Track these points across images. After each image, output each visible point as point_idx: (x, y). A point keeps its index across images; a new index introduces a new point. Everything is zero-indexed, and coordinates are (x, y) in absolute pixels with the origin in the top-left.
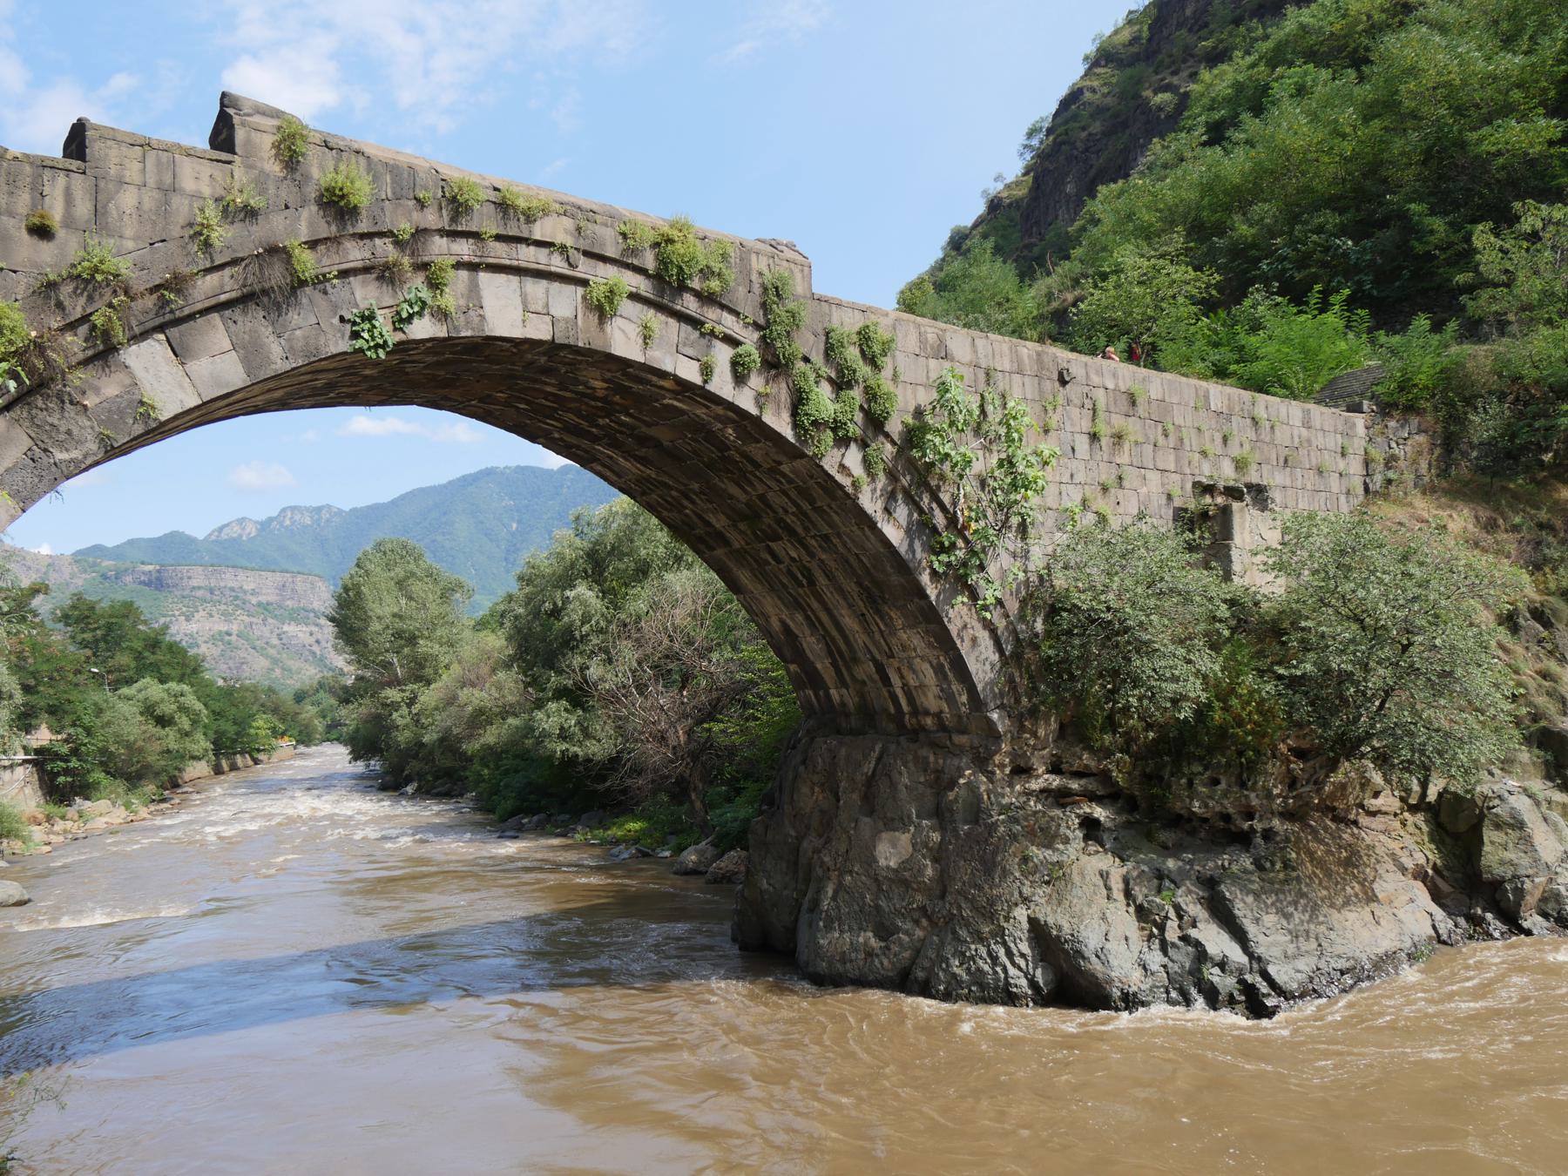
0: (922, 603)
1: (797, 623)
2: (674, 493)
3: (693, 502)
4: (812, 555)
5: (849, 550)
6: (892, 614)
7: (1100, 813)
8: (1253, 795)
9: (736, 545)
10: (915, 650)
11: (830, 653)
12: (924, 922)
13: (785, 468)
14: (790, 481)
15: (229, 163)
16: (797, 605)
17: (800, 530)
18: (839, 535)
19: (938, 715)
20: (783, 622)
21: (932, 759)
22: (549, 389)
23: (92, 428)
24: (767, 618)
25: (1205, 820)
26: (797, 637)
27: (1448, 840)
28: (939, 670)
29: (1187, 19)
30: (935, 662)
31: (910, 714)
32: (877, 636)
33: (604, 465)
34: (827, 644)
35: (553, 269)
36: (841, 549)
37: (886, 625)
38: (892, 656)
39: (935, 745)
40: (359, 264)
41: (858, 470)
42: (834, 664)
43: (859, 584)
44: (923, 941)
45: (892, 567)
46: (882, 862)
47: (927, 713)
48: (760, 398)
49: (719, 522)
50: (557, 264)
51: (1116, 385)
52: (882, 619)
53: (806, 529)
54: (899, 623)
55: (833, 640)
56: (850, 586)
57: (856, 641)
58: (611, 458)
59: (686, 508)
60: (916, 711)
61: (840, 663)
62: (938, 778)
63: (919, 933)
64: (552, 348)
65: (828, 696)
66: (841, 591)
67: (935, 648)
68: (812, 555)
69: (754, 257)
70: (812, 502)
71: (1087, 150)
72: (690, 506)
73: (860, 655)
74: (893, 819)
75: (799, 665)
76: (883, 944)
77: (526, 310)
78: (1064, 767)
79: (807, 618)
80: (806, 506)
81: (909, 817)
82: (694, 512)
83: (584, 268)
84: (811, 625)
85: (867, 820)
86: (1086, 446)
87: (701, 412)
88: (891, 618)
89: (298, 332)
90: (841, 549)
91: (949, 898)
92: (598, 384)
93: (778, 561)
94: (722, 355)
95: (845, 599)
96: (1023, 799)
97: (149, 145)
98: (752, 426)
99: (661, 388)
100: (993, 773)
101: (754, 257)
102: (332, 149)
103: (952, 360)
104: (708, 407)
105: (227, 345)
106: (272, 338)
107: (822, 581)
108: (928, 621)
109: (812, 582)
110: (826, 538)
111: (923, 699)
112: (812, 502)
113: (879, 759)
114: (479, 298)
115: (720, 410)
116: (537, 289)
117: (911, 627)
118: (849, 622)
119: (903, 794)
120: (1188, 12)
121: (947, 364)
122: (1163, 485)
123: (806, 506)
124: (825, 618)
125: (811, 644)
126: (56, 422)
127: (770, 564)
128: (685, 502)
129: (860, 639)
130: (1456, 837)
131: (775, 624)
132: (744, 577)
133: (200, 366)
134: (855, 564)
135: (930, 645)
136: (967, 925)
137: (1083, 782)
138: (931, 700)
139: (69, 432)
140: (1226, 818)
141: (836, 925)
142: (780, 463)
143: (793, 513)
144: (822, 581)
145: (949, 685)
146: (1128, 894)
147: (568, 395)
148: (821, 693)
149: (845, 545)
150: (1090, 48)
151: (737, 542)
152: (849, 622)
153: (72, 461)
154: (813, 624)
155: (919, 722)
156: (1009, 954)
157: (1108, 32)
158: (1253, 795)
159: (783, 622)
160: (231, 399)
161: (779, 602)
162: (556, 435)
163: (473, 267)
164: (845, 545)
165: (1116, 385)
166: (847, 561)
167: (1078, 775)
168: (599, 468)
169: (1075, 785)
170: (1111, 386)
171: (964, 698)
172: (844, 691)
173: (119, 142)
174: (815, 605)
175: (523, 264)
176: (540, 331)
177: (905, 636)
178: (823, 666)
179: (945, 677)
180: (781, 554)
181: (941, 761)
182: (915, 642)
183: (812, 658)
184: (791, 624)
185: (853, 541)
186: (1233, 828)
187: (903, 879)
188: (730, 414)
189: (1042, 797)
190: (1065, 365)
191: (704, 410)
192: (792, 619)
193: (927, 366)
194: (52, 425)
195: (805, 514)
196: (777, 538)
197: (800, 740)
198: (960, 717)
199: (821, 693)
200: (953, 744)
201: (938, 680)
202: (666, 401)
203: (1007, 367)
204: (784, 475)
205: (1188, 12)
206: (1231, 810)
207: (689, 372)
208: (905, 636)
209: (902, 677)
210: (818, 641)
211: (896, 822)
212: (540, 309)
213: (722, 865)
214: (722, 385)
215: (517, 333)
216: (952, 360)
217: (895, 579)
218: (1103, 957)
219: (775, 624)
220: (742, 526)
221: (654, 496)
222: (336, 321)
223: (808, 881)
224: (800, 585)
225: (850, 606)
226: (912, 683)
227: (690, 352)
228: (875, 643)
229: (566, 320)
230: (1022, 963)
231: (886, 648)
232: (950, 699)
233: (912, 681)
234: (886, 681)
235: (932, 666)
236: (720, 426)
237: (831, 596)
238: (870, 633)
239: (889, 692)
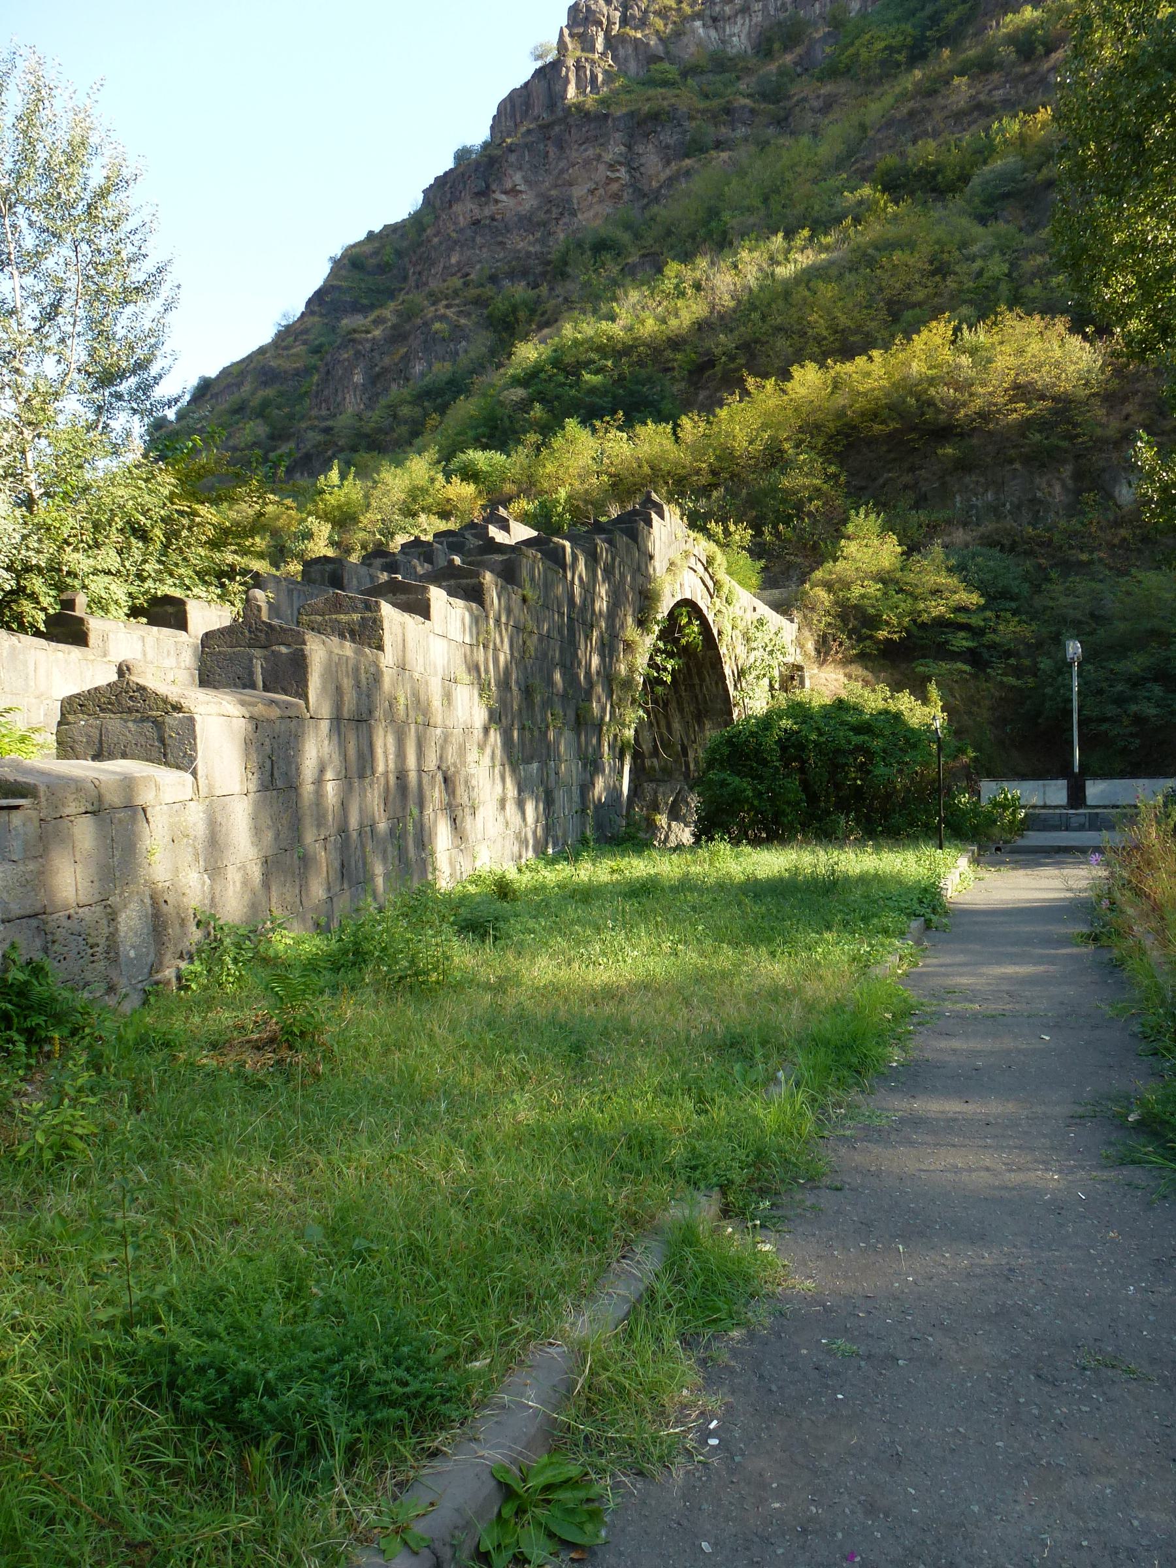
18: (701, 686)
29: (451, 265)
38: (694, 742)
52: (699, 725)
54: (708, 726)
56: (689, 708)
66: (681, 711)
71: (372, 350)
80: (694, 671)
90: (698, 691)
107: (673, 705)
113: (678, 794)
120: (453, 260)
123: (694, 671)
144: (673, 705)
150: (338, 253)
166: (696, 697)
172: (655, 760)
205: (453, 260)
228: (687, 735)
234: (685, 754)
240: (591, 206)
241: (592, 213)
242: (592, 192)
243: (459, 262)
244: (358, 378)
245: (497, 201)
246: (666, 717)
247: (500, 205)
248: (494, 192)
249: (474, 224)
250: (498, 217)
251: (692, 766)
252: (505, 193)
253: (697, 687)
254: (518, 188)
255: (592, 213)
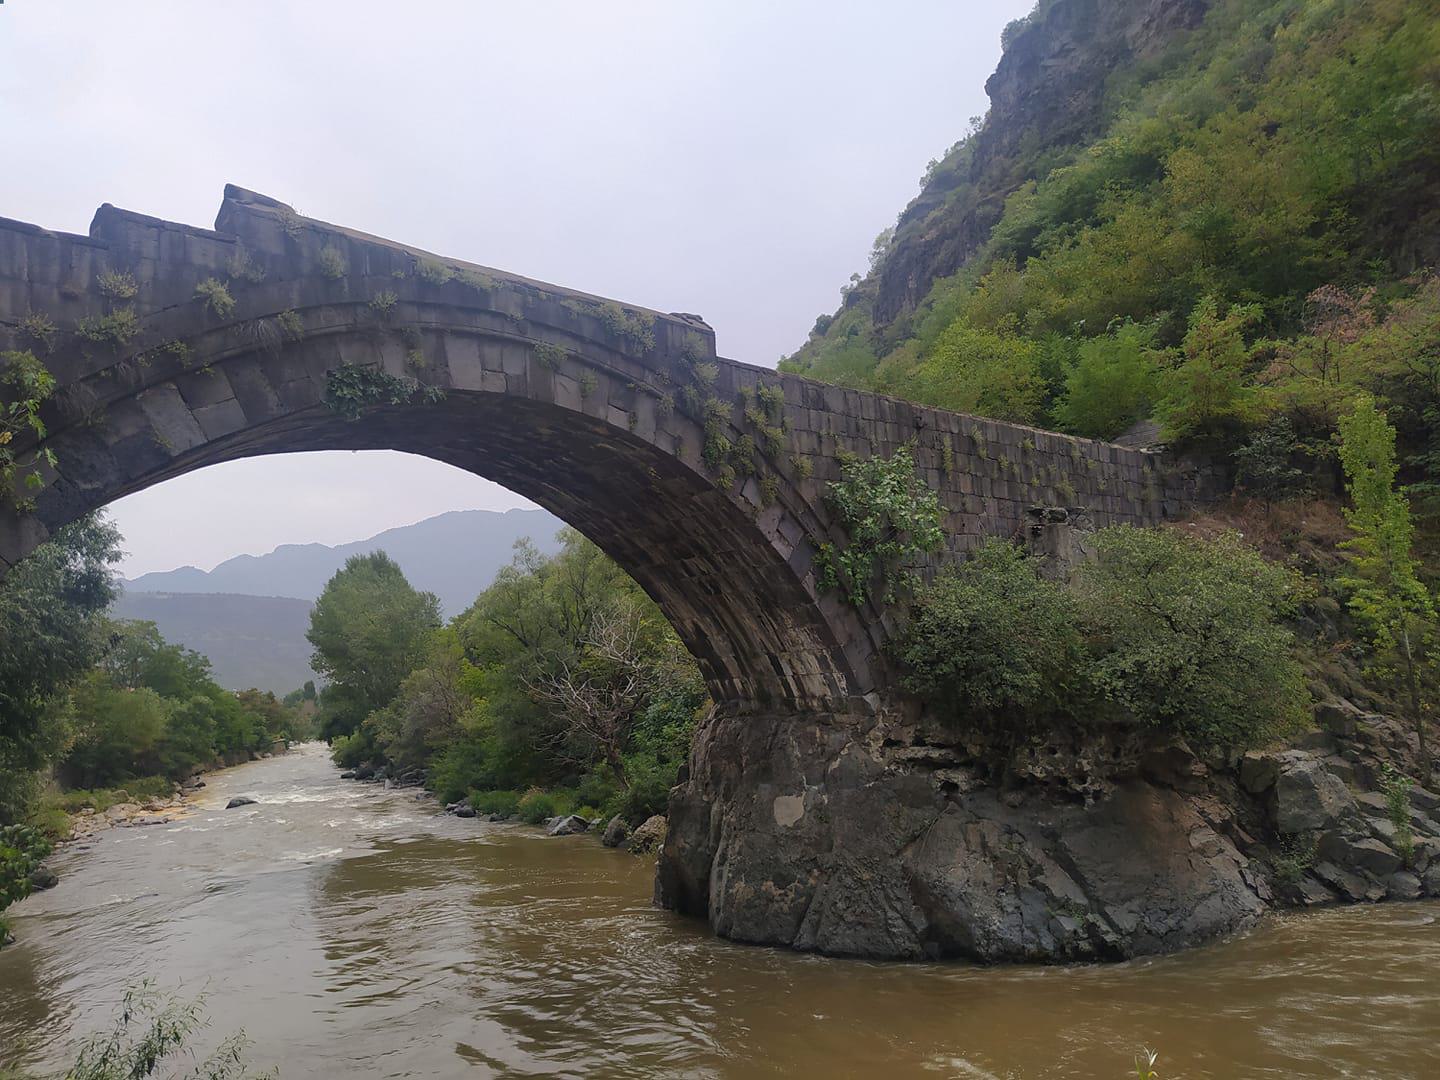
0: (808, 606)
1: (707, 625)
2: (606, 520)
3: (621, 527)
4: (717, 568)
5: (748, 565)
6: (784, 617)
7: (959, 778)
8: (1084, 762)
9: (658, 563)
10: (803, 644)
11: (734, 650)
12: (816, 872)
13: (696, 498)
14: (700, 509)
15: (233, 242)
16: (704, 610)
17: (710, 550)
19: (822, 699)
20: (694, 623)
21: (818, 734)
22: (503, 435)
23: (113, 463)
24: (682, 622)
25: (1046, 783)
26: (707, 636)
27: (1248, 799)
28: (822, 661)
30: (819, 655)
31: (800, 697)
32: (771, 631)
33: (549, 499)
34: (732, 643)
35: (506, 335)
36: (743, 564)
37: (778, 625)
39: (824, 723)
40: (344, 329)
41: (755, 501)
42: (737, 658)
43: (756, 591)
44: (813, 888)
45: (783, 578)
46: (781, 823)
47: (814, 697)
48: (677, 442)
49: (643, 544)
50: (510, 332)
51: (960, 431)
52: (775, 620)
53: (715, 548)
54: (789, 622)
55: (738, 641)
56: (751, 596)
57: (755, 640)
58: (553, 491)
59: (616, 532)
60: (803, 695)
61: (742, 657)
62: (823, 751)
63: (812, 881)
64: (506, 399)
65: (732, 683)
66: (740, 596)
67: (818, 643)
68: (717, 568)
69: (669, 327)
70: (718, 525)
72: (620, 531)
73: (759, 650)
74: (787, 786)
75: (708, 660)
76: (783, 892)
77: (484, 368)
78: (928, 740)
79: (715, 620)
80: (713, 529)
81: (801, 783)
82: (621, 535)
83: (531, 336)
84: (720, 630)
85: (767, 785)
86: (937, 480)
87: (628, 453)
88: (782, 618)
89: (291, 384)
91: (835, 851)
92: (545, 431)
93: (691, 574)
94: (645, 409)
95: (745, 603)
96: (893, 767)
97: (163, 227)
98: (670, 465)
99: (596, 433)
100: (869, 745)
101: (669, 327)
102: (319, 233)
103: (829, 411)
104: (634, 449)
105: (230, 393)
106: (268, 388)
107: (726, 590)
108: (813, 621)
109: (718, 591)
110: (730, 555)
111: (810, 685)
112: (718, 525)
114: (445, 358)
115: (644, 452)
116: (492, 353)
117: (798, 626)
118: (749, 623)
119: (796, 765)
120: (1005, 141)
121: (824, 413)
122: (999, 510)
124: (728, 620)
125: (718, 643)
126: (80, 457)
127: (683, 576)
128: (616, 528)
129: (758, 637)
130: (1255, 796)
131: (689, 625)
132: (663, 588)
133: (207, 411)
134: (753, 576)
135: (814, 640)
136: (850, 872)
137: (943, 752)
138: (816, 686)
139: (92, 467)
140: (1064, 781)
141: (743, 876)
142: (693, 494)
143: (703, 535)
145: (831, 674)
146: (984, 845)
147: (521, 440)
148: (726, 682)
149: (744, 560)
151: (658, 560)
152: (749, 623)
153: (94, 490)
154: (720, 625)
155: (806, 704)
156: (887, 897)
157: (940, 159)
158: (1084, 762)
159: (694, 623)
160: (234, 440)
161: (692, 609)
162: (509, 474)
163: (440, 333)
164: (744, 560)
165: (960, 431)
167: (939, 746)
168: (546, 501)
169: (935, 754)
170: (956, 431)
171: (843, 684)
173: (136, 222)
174: (721, 608)
175: (483, 331)
176: (496, 385)
177: (794, 634)
178: (728, 659)
179: (828, 667)
180: (694, 569)
181: (826, 737)
182: (803, 638)
183: (717, 652)
184: (701, 625)
185: (751, 557)
186: (1068, 789)
187: (793, 835)
188: (652, 454)
189: (910, 765)
190: (918, 414)
191: (632, 452)
192: (702, 622)
193: (809, 416)
194: (77, 460)
195: (712, 536)
196: (690, 556)
197: (710, 721)
198: (840, 699)
199: (726, 682)
200: (835, 722)
201: (822, 669)
202: (599, 445)
203: (872, 416)
204: (695, 504)
206: (1067, 775)
207: (618, 419)
208: (794, 634)
209: (792, 667)
210: (724, 639)
211: (793, 788)
212: (496, 367)
213: (646, 829)
214: (645, 430)
215: (477, 387)
216: (829, 411)
217: (786, 587)
218: (967, 901)
219: (689, 625)
220: (662, 547)
221: (590, 523)
222: (324, 375)
223: (717, 839)
224: (709, 592)
225: (750, 610)
226: (800, 672)
227: (620, 404)
229: (518, 377)
230: (898, 906)
231: (780, 645)
232: (832, 684)
233: (801, 671)
235: (816, 657)
236: (644, 465)
237: (731, 601)
238: (765, 632)
239: (782, 680)
240: (1146, 43)
241: (1150, 47)
242: (1147, 26)
243: (1010, 143)
244: (912, 285)
245: (1046, 68)
246: (727, 608)
247: (1049, 71)
248: (1042, 59)
249: (1023, 99)
250: (1050, 83)
251: (794, 688)
252: (1054, 57)
253: (738, 557)
254: (1067, 47)
255: (1150, 47)
